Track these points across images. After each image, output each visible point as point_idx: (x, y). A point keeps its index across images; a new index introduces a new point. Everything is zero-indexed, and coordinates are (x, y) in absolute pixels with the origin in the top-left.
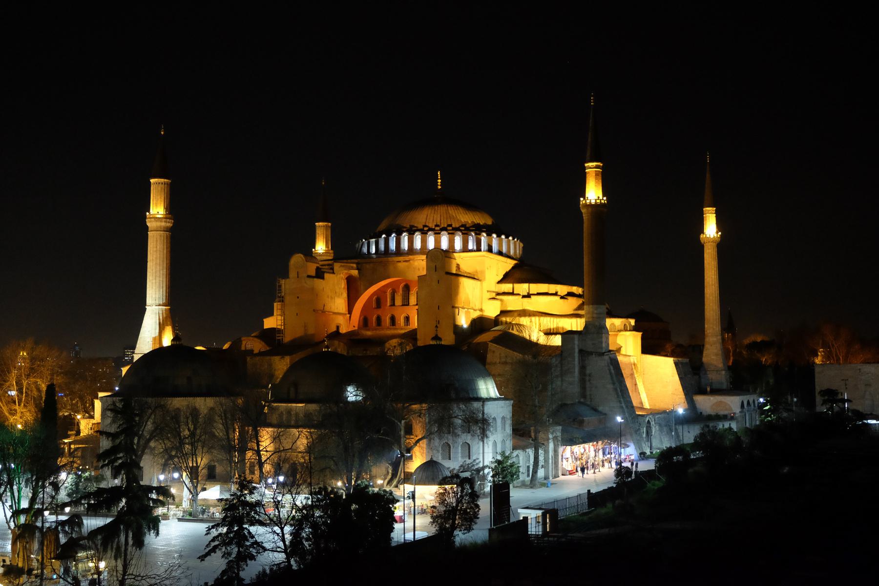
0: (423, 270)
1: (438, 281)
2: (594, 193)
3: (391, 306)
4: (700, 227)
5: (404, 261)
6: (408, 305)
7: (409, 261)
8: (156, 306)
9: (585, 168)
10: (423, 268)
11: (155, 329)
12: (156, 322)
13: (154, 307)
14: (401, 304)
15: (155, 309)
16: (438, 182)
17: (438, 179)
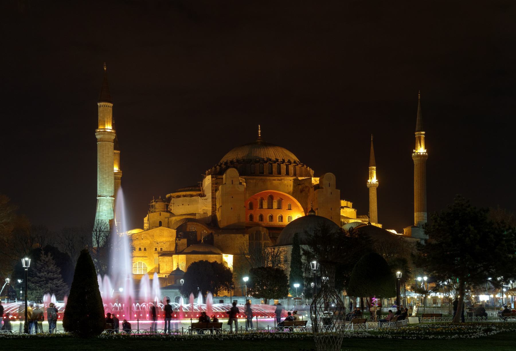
0: (290, 187)
1: (331, 193)
2: (421, 150)
3: (260, 208)
4: (367, 176)
5: (278, 180)
6: (272, 208)
7: (281, 180)
8: (110, 197)
9: (415, 135)
10: (290, 185)
11: (111, 214)
12: (111, 209)
13: (108, 198)
14: (267, 208)
15: (109, 199)
16: (259, 132)
17: (259, 130)
